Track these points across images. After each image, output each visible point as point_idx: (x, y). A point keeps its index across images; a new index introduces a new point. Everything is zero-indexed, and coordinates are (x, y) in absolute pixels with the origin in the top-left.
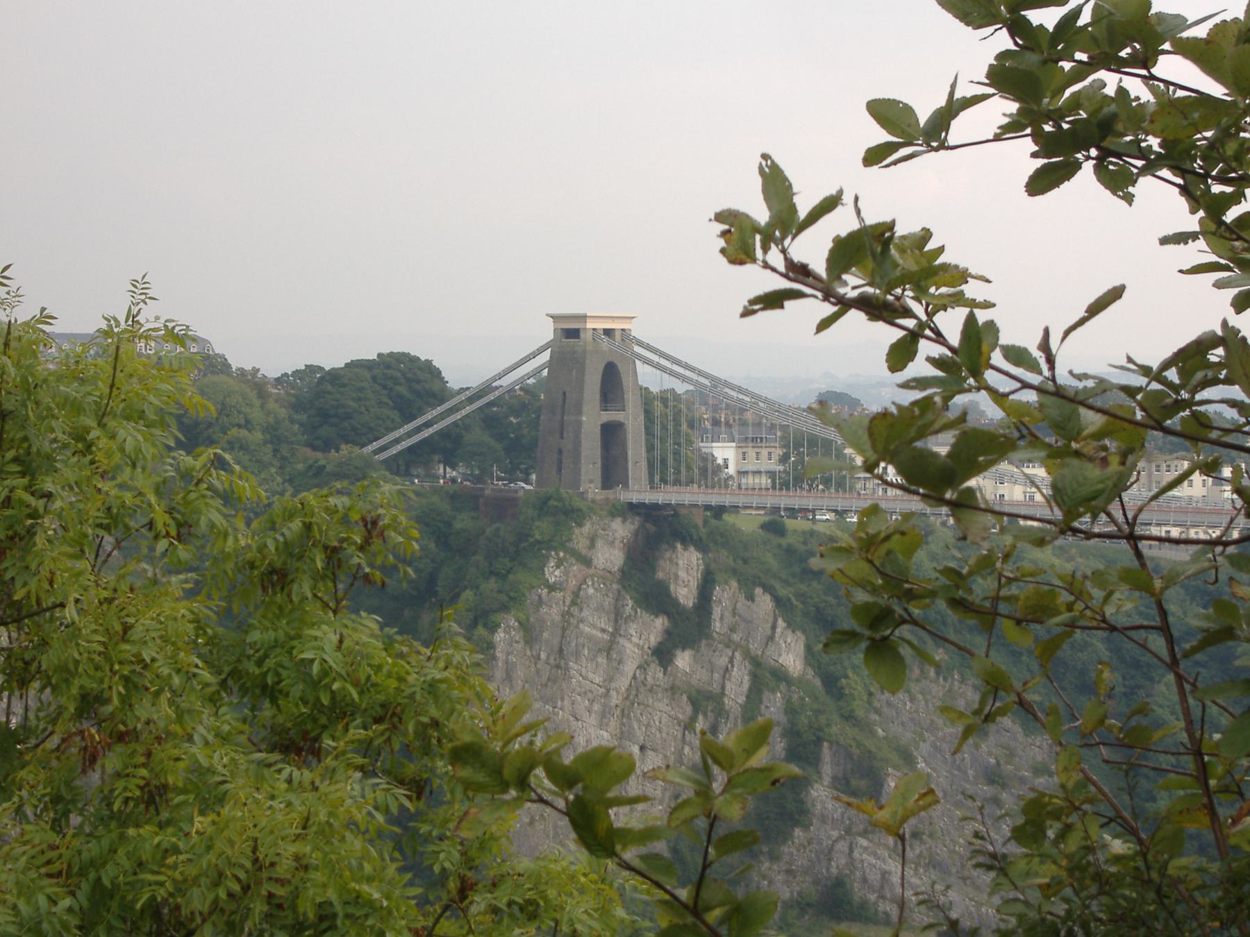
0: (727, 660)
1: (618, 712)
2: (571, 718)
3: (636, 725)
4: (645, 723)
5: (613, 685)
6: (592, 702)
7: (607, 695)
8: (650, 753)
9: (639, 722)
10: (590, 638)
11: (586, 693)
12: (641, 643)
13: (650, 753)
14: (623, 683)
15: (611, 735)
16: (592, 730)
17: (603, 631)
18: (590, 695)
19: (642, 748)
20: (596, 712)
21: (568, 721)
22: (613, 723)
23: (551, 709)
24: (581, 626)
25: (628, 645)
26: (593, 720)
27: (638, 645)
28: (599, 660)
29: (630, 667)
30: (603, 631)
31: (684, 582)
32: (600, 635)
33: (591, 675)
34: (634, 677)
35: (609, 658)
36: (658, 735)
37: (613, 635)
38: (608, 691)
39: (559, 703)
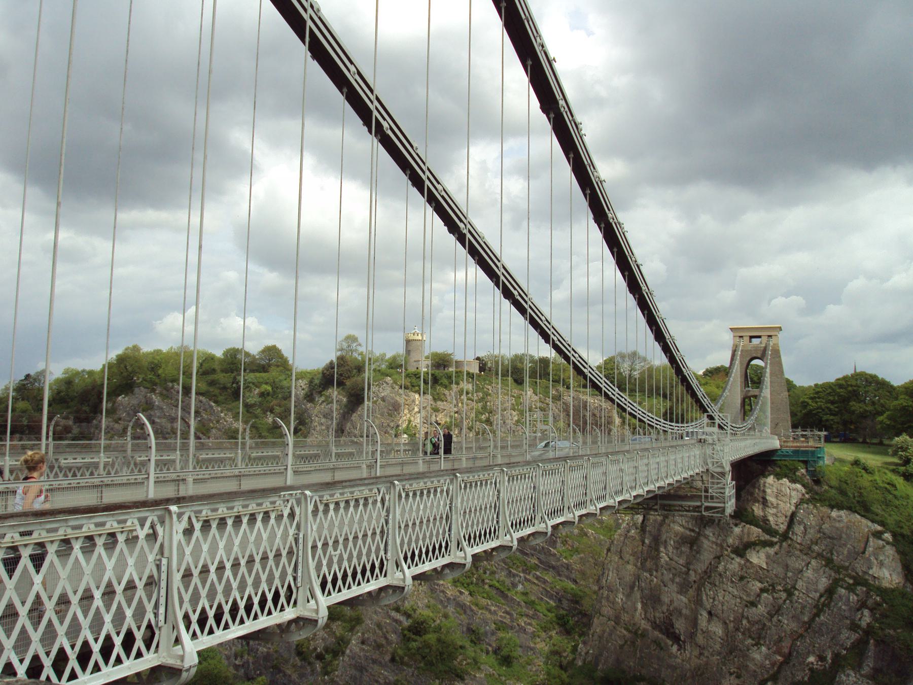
0: (803, 564)
1: (695, 586)
2: (662, 584)
3: (704, 598)
4: (712, 596)
5: (691, 567)
6: (674, 575)
7: (687, 573)
8: (715, 618)
9: (707, 595)
10: (676, 534)
11: (670, 569)
12: (719, 542)
13: (715, 618)
14: (700, 567)
15: (690, 601)
16: (674, 595)
17: (693, 531)
18: (674, 571)
19: (710, 613)
20: (677, 583)
21: (660, 585)
22: (691, 592)
23: (648, 575)
24: (672, 525)
25: (705, 542)
26: (674, 588)
27: (713, 542)
28: (683, 549)
29: (707, 556)
30: (693, 531)
31: (772, 504)
32: (688, 533)
33: (676, 558)
34: (710, 564)
35: (691, 548)
36: (720, 606)
37: (699, 534)
38: (689, 570)
39: (655, 573)
